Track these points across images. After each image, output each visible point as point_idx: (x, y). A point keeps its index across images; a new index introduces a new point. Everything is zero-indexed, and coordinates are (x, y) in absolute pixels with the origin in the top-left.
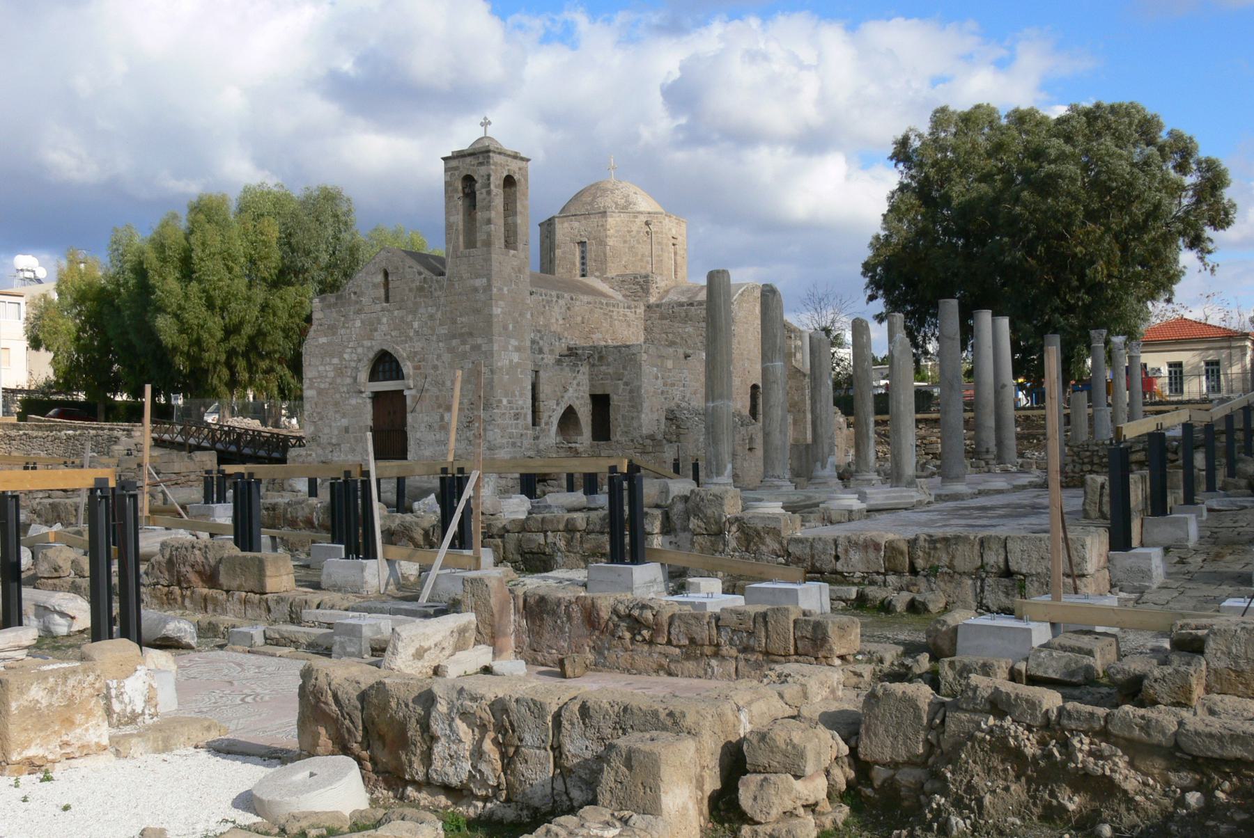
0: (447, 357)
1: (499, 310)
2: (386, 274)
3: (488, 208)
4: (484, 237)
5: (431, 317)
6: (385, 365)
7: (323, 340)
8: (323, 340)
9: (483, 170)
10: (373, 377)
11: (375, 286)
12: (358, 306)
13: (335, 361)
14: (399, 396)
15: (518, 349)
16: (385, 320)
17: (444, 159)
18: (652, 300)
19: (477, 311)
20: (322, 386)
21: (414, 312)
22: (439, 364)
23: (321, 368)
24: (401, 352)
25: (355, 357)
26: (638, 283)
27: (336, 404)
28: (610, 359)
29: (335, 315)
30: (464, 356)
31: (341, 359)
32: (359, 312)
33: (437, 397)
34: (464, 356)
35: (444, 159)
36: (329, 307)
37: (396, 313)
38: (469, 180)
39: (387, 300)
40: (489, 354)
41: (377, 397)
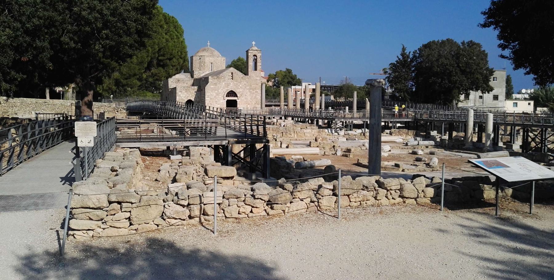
0: (249, 93)
2: (232, 73)
6: (232, 93)
10: (227, 96)
21: (240, 83)
24: (236, 91)
27: (216, 102)
30: (253, 93)
34: (253, 93)
39: (232, 79)
41: (228, 102)
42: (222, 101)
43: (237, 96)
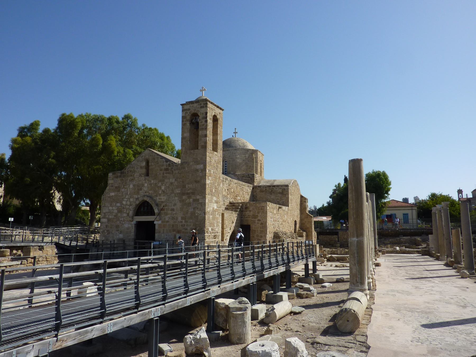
0: (179, 205)
1: (209, 181)
2: (148, 162)
3: (206, 129)
4: (203, 144)
5: (172, 183)
6: (144, 208)
7: (113, 194)
8: (113, 194)
9: (203, 110)
11: (141, 168)
12: (132, 178)
13: (118, 205)
14: (151, 224)
15: (217, 202)
16: (146, 185)
17: (182, 105)
18: (255, 184)
19: (197, 182)
20: (110, 217)
21: (162, 181)
22: (175, 208)
23: (110, 208)
25: (128, 203)
26: (249, 177)
27: (117, 227)
28: (251, 209)
29: (120, 181)
31: (121, 203)
32: (132, 180)
33: (173, 226)
34: (189, 204)
35: (182, 105)
36: (117, 177)
37: (152, 181)
38: (195, 116)
39: (147, 174)
40: (203, 205)
41: (139, 225)
42: (126, 226)
43: (152, 213)
